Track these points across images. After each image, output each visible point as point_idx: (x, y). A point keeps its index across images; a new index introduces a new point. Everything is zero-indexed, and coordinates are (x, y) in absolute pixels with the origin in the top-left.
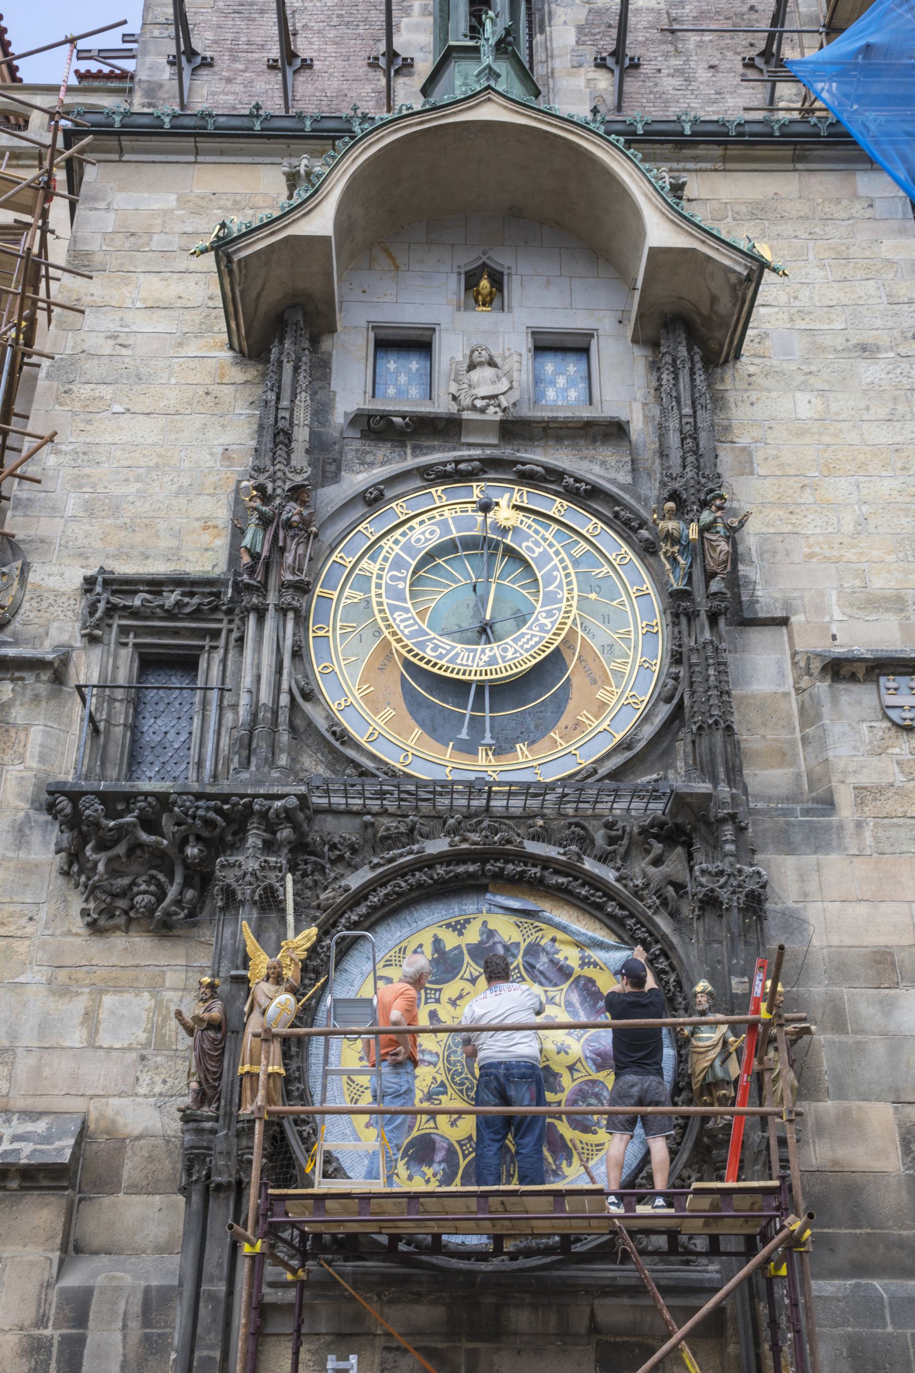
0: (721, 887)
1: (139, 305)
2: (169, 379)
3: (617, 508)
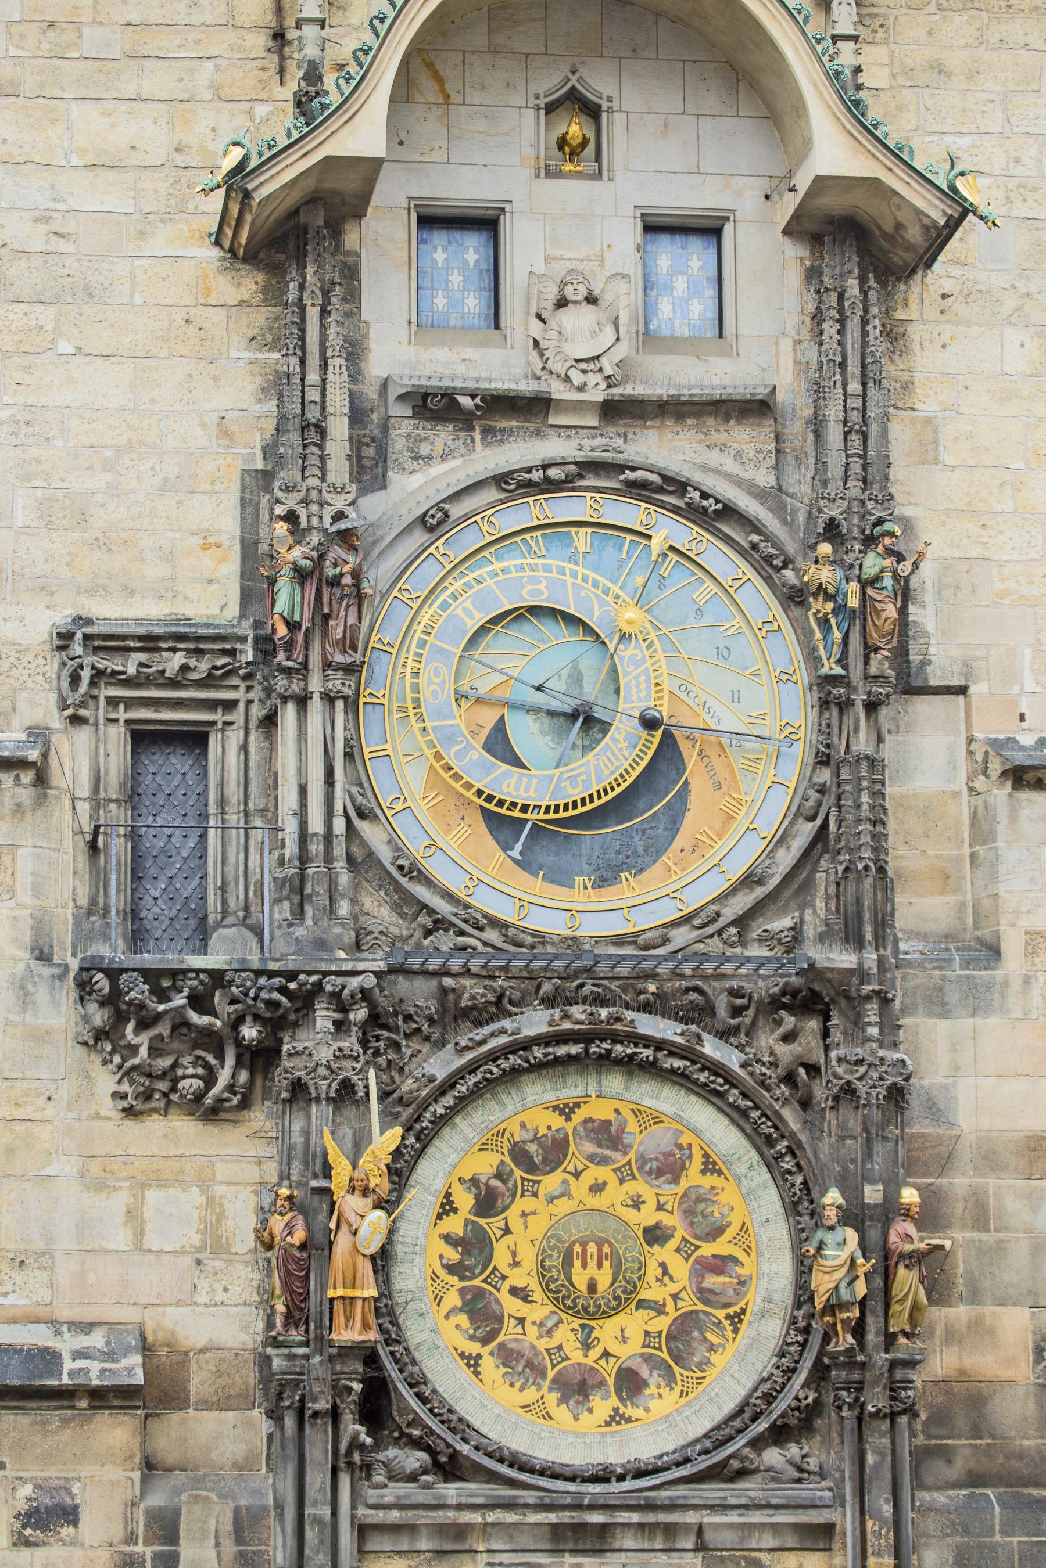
0: (860, 1079)
1: (75, 161)
3: (755, 538)
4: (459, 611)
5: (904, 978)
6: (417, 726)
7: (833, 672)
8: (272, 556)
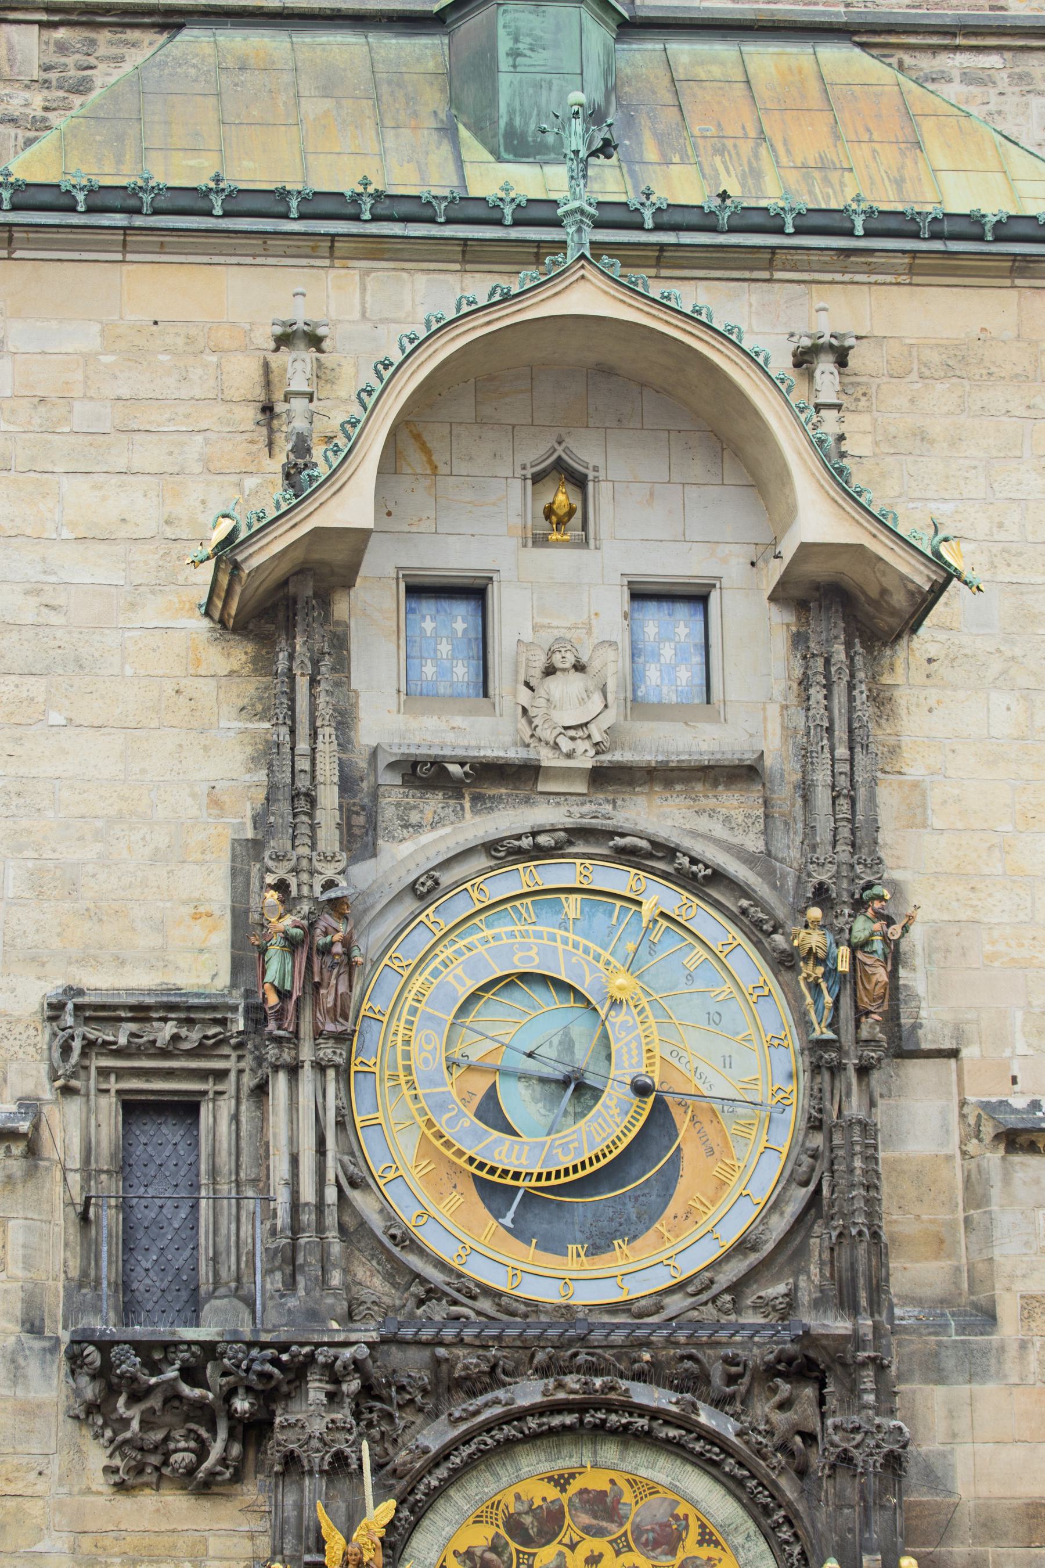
0: (857, 1447)
1: (66, 534)
2: (123, 667)
3: (745, 903)
4: (450, 978)
5: (900, 1344)
6: (408, 1093)
7: (824, 1037)
8: (262, 925)
